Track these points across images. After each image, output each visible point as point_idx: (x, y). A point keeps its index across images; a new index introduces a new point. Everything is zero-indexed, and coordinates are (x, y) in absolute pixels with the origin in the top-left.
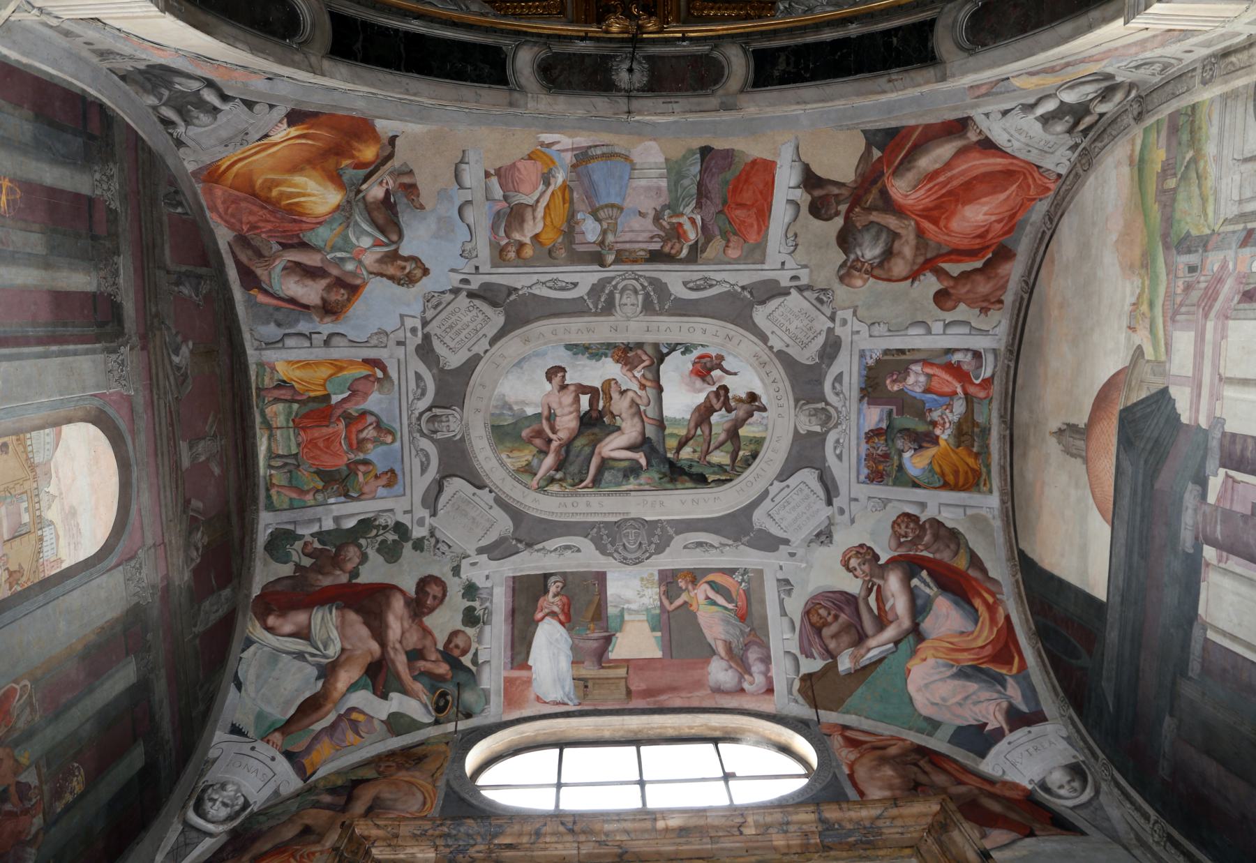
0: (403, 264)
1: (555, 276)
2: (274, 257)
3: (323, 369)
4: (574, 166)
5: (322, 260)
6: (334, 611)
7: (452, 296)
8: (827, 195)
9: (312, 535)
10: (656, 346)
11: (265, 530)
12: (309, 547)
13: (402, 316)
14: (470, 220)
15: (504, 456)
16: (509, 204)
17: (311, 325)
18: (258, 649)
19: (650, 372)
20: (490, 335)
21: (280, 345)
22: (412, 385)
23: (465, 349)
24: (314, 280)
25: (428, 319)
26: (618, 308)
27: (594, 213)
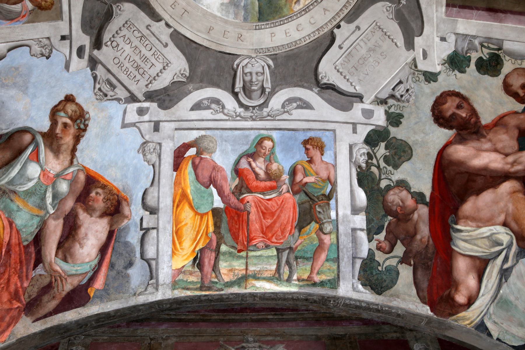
0: (60, 127)
2: (52, 273)
3: (183, 215)
5: (56, 218)
6: (459, 227)
7: (100, 67)
9: (370, 240)
11: (359, 292)
12: (383, 245)
13: (124, 126)
15: (297, 8)
17: (132, 229)
18: (490, 318)
20: (147, 20)
21: (153, 263)
22: (206, 114)
23: (164, 51)
24: (79, 227)
25: (129, 95)
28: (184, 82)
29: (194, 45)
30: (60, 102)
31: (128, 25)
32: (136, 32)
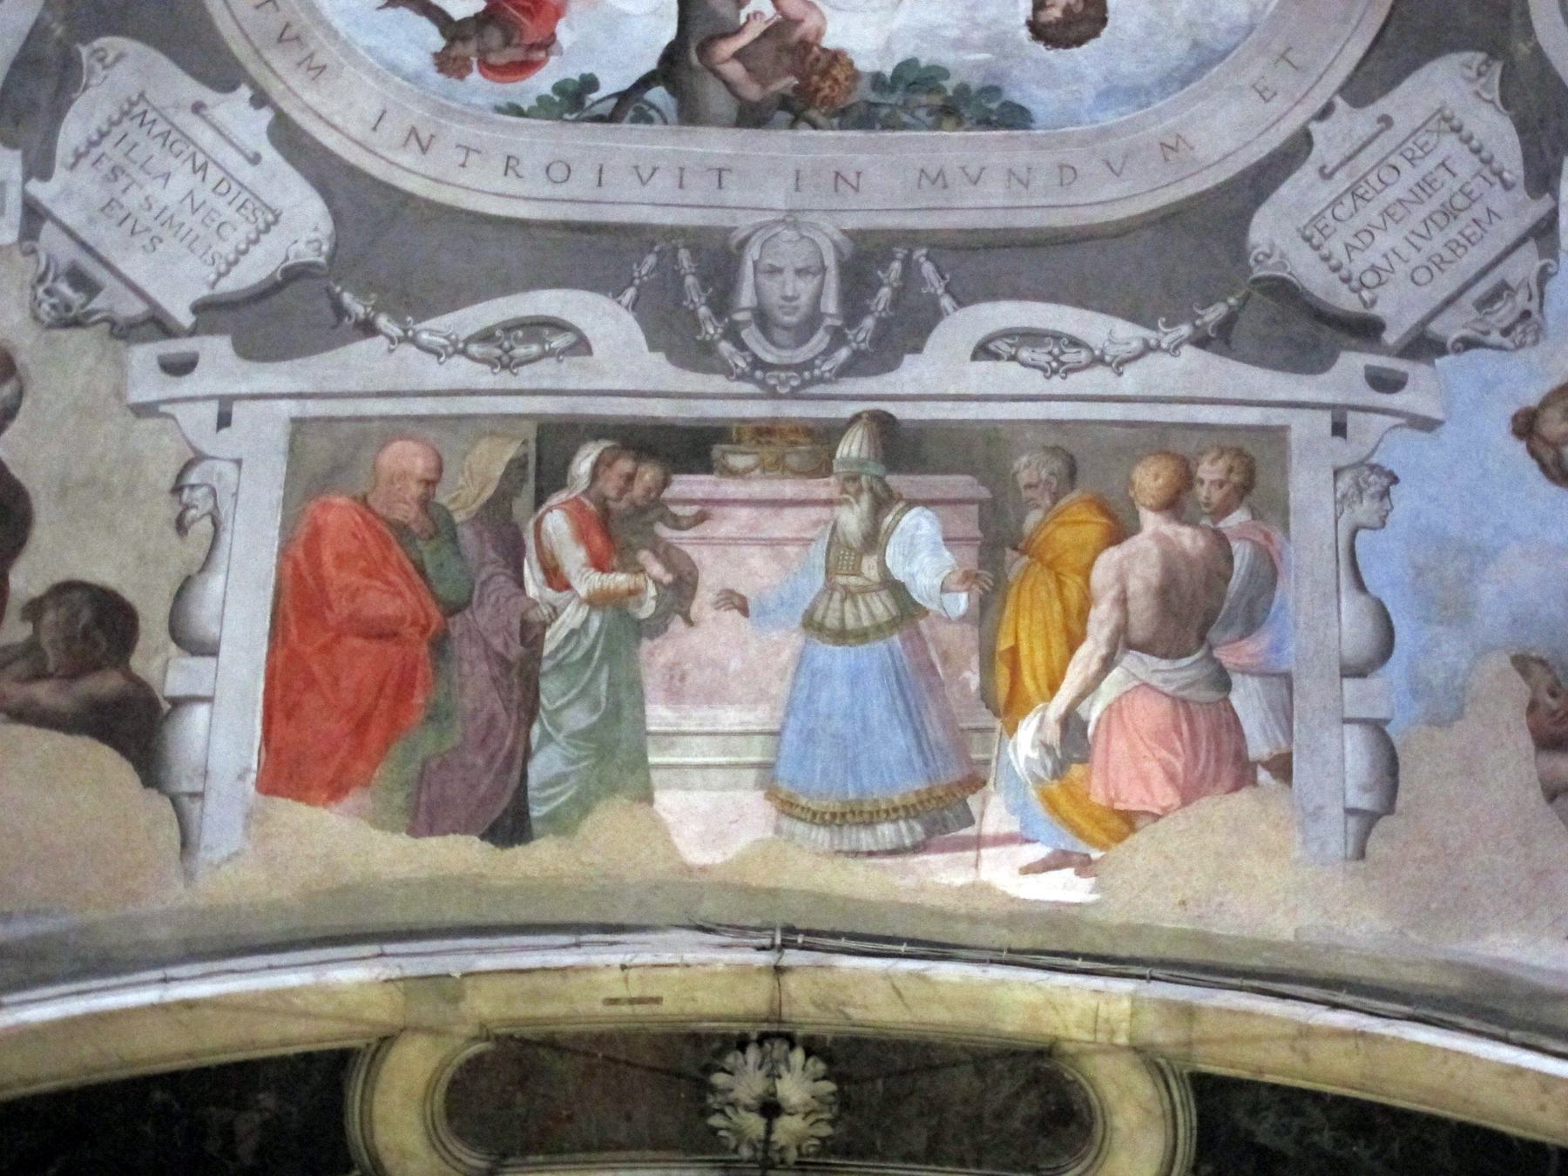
1: (1057, 385)
4: (975, 783)
7: (1435, 327)
8: (75, 672)
10: (690, 114)
14: (1351, 608)
16: (1210, 658)
19: (713, 15)
20: (1306, 174)
23: (1402, 127)
25: (1531, 245)
26: (830, 260)
27: (907, 609)
28: (1504, 68)
29: (1391, 34)
30: (1533, 453)
31: (1317, 234)
32: (1339, 212)
